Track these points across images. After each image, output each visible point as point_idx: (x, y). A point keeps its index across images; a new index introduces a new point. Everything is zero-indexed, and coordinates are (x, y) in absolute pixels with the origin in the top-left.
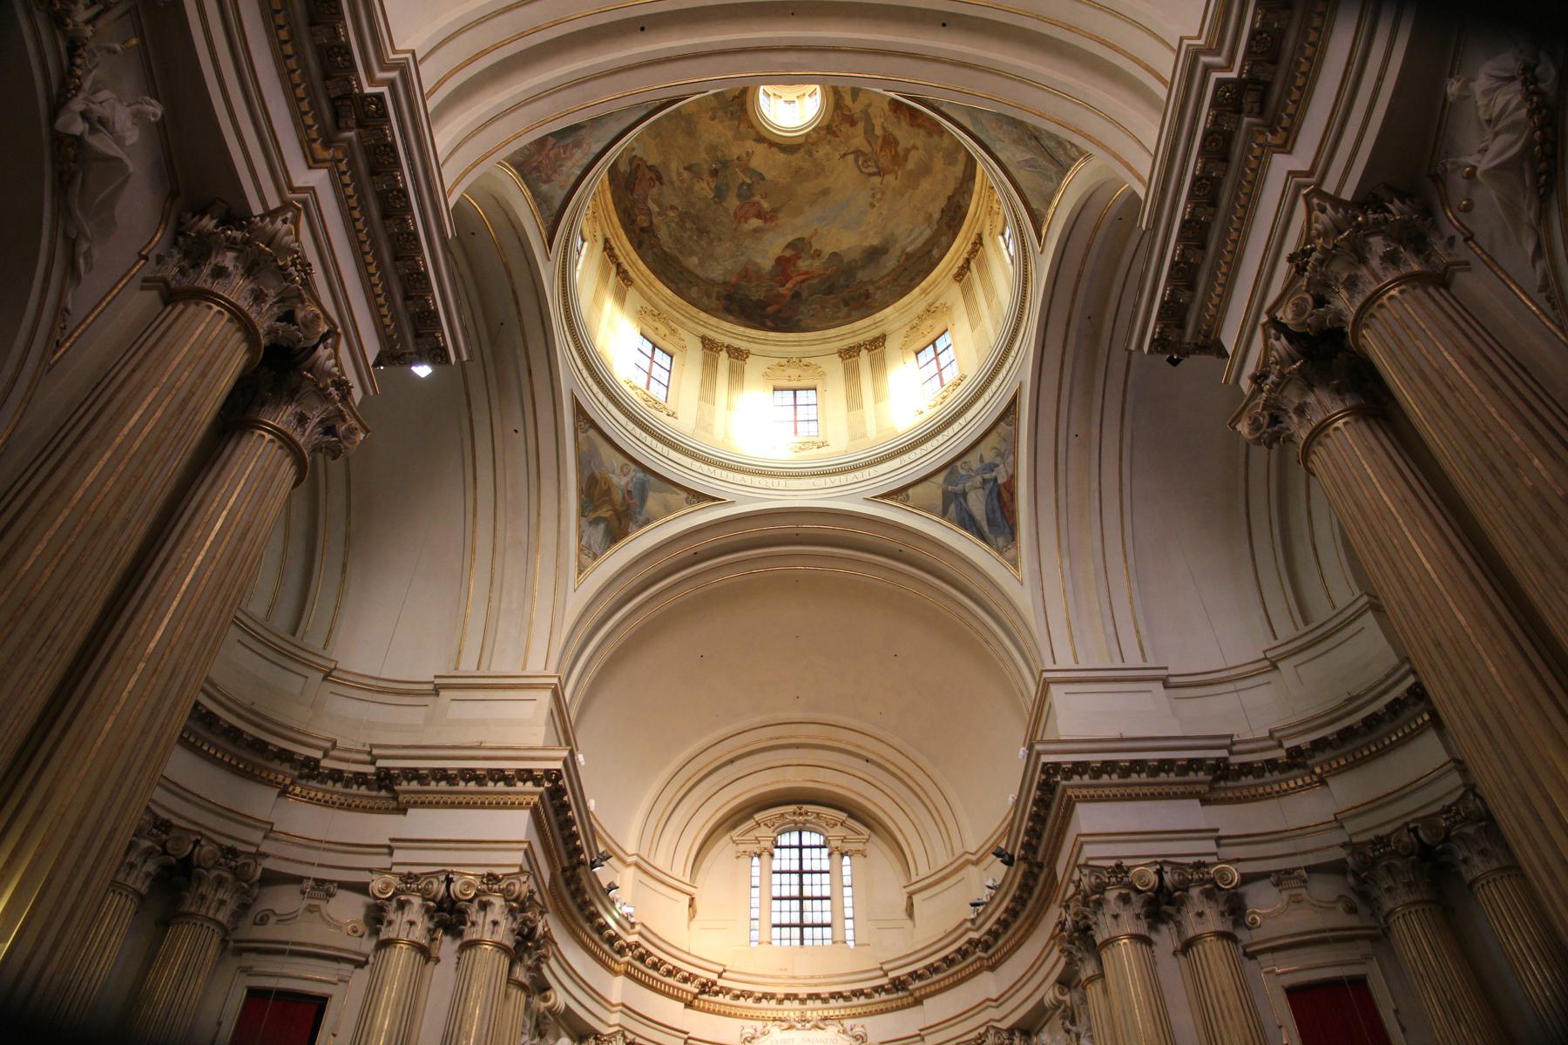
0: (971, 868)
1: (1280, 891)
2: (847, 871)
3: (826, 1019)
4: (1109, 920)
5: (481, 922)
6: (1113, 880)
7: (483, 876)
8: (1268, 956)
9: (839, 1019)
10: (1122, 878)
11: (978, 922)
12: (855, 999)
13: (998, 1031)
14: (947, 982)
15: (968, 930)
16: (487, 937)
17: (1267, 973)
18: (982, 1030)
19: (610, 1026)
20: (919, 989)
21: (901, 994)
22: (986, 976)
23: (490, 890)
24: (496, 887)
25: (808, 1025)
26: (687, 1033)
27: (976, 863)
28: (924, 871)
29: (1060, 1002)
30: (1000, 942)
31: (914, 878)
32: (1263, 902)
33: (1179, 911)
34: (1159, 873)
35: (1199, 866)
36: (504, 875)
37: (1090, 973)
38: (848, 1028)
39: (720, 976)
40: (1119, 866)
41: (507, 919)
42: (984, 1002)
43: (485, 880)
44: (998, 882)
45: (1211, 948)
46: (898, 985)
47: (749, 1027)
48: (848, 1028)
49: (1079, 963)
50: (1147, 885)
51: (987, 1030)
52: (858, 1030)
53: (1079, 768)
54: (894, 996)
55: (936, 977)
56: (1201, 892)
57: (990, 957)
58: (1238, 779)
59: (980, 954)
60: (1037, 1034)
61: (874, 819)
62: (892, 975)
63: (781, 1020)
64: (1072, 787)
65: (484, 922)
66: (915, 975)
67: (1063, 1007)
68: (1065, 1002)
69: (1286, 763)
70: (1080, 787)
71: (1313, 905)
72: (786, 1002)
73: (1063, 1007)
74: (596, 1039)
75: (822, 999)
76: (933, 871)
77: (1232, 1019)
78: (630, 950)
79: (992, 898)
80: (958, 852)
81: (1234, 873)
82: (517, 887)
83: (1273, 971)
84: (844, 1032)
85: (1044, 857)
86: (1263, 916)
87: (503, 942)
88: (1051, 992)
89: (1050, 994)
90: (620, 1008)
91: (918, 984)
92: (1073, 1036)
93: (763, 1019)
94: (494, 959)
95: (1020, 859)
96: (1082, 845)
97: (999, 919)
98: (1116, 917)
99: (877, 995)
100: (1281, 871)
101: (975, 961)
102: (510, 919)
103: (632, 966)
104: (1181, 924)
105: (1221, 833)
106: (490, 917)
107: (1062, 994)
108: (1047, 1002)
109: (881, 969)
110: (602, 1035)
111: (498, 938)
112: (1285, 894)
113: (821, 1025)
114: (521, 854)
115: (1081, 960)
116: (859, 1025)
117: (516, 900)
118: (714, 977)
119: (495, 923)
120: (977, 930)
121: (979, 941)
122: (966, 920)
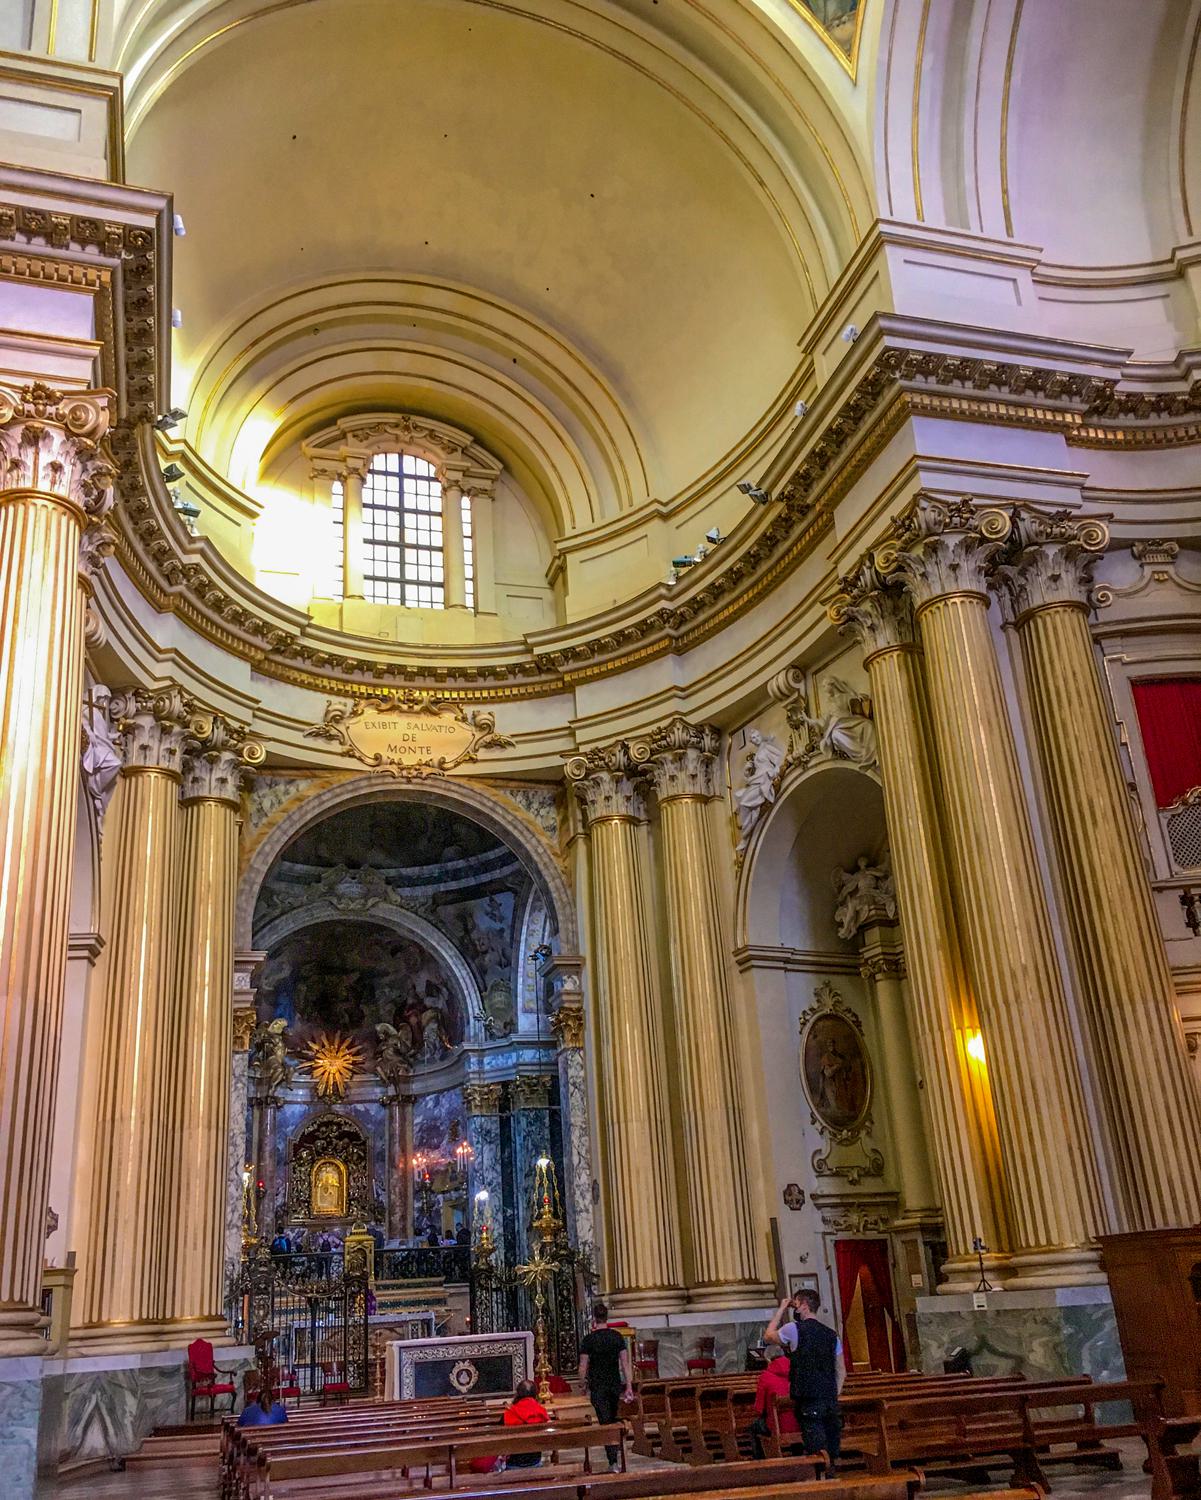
0: (656, 523)
1: (1142, 566)
2: (466, 516)
3: (437, 702)
4: (944, 570)
5: (30, 462)
6: (956, 520)
7: (24, 390)
8: (1118, 641)
9: (456, 703)
10: (967, 519)
11: (675, 591)
12: (481, 679)
13: (686, 726)
14: (617, 664)
15: (661, 597)
16: (44, 486)
17: (1110, 661)
18: (664, 724)
19: (156, 679)
20: (571, 671)
21: (544, 677)
22: (669, 663)
23: (40, 414)
24: (51, 410)
25: (417, 708)
26: (257, 702)
27: (665, 517)
28: (584, 522)
29: (792, 690)
30: (702, 617)
31: (569, 532)
32: (1118, 574)
33: (1023, 573)
34: (1015, 519)
35: (1064, 516)
36: (65, 393)
37: (882, 644)
38: (469, 716)
39: (304, 634)
40: (965, 502)
41: (74, 465)
42: (670, 690)
43: (29, 397)
44: (723, 535)
45: (1062, 621)
46: (546, 665)
47: (339, 703)
48: (469, 716)
49: (866, 632)
50: (997, 533)
51: (673, 724)
52: (483, 717)
53: (928, 365)
54: (536, 679)
55: (598, 658)
56: (1061, 551)
57: (681, 637)
58: (1116, 416)
59: (668, 630)
60: (732, 734)
61: (513, 451)
62: (537, 651)
63: (385, 699)
64: (913, 390)
65: (36, 464)
66: (571, 654)
67: (796, 695)
68: (798, 690)
69: (1185, 402)
70: (921, 392)
71: (1179, 585)
72: (386, 675)
73: (796, 695)
74: (136, 694)
75: (435, 675)
76: (598, 524)
77: (1081, 705)
78: (185, 576)
79: (706, 557)
80: (638, 502)
81: (1105, 532)
82: (92, 416)
83: (1120, 659)
84: (464, 719)
85: (818, 499)
86: (1118, 595)
87: (72, 498)
88: (781, 677)
89: (777, 679)
90: (173, 655)
91: (572, 665)
92: (804, 731)
93: (353, 695)
94: (59, 524)
95: (781, 497)
96: (917, 469)
97: (713, 584)
98: (954, 567)
99: (511, 677)
100: (1149, 540)
101: (660, 640)
102: (79, 466)
103: (186, 600)
104: (1023, 588)
105: (1088, 483)
106: (45, 458)
107: (797, 680)
108: (772, 688)
109: (525, 643)
110: (147, 690)
111: (62, 491)
112: (1148, 570)
113: (435, 709)
114: (88, 365)
115: (872, 628)
116: (484, 712)
117: (90, 434)
118: (296, 631)
119: (56, 468)
120: (671, 599)
121: (672, 614)
122: (661, 584)
